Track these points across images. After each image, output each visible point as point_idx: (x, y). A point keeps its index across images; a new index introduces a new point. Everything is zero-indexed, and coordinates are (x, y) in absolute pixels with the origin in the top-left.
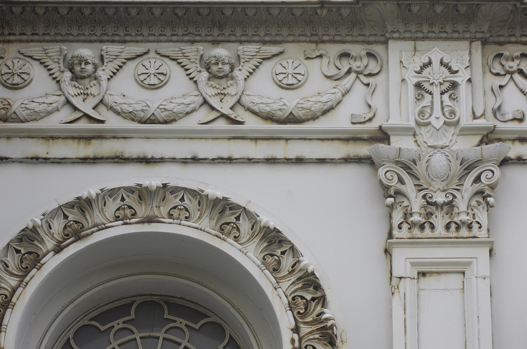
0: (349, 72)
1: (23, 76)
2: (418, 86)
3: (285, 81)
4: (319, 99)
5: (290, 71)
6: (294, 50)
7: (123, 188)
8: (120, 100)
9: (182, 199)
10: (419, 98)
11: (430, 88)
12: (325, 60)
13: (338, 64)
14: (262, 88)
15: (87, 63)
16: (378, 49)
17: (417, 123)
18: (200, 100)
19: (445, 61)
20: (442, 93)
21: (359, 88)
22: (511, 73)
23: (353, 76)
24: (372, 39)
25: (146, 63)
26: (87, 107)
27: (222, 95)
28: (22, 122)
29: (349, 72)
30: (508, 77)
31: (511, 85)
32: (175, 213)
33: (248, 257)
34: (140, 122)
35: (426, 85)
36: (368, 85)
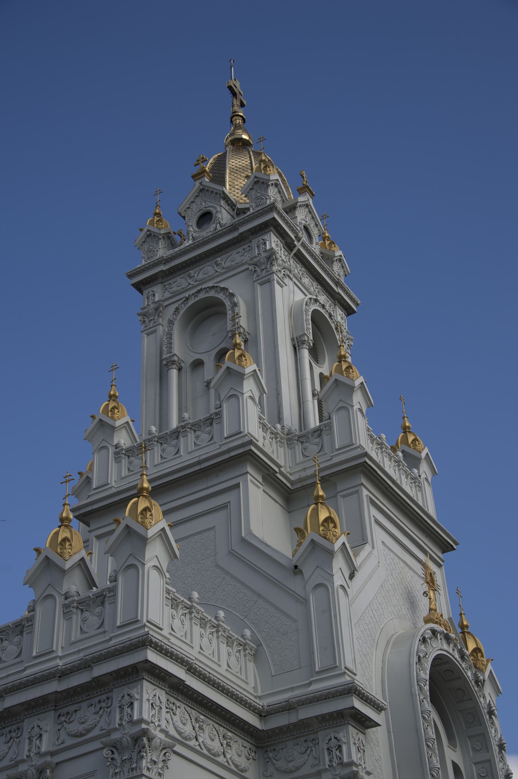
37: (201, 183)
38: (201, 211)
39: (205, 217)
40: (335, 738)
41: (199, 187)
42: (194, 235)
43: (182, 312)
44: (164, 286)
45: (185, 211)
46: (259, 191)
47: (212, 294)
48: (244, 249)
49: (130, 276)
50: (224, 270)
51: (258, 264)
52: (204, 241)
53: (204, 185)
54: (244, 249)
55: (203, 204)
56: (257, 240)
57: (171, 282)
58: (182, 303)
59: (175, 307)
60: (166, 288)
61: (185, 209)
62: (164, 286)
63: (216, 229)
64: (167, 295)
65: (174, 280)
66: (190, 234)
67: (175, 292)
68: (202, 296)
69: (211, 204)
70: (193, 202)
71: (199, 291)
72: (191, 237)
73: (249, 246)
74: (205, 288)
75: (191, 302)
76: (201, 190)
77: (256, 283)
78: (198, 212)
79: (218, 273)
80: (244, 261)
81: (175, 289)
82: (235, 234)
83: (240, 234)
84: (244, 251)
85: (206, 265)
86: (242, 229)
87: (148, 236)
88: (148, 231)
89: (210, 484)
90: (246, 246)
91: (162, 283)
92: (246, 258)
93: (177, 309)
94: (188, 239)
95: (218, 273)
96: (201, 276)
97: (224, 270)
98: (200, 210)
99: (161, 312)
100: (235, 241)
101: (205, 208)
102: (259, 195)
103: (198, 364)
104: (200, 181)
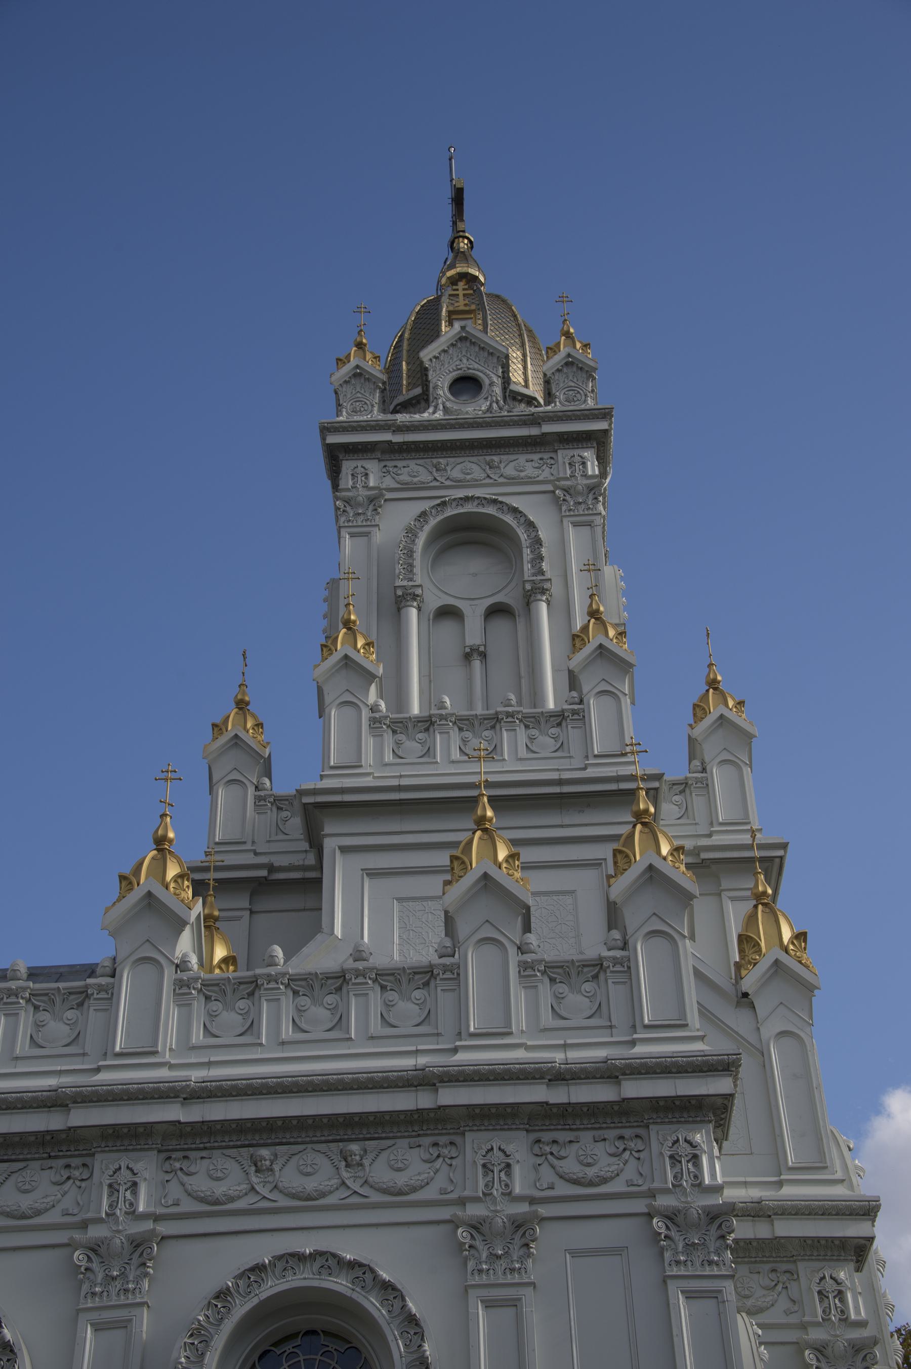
0: (438, 1156)
1: (224, 1171)
2: (484, 1166)
3: (396, 1166)
4: (418, 1177)
5: (400, 1158)
6: (403, 1143)
7: (288, 1254)
8: (287, 1185)
9: (327, 1260)
10: (485, 1175)
11: (491, 1167)
12: (422, 1149)
13: (431, 1150)
14: (380, 1171)
15: (265, 1160)
16: (458, 1139)
17: (483, 1193)
18: (339, 1181)
19: (502, 1147)
20: (500, 1171)
21: (445, 1167)
22: (546, 1155)
23: (441, 1159)
24: (451, 1131)
25: (305, 1157)
26: (265, 1192)
27: (356, 1178)
28: (222, 1204)
29: (438, 1156)
30: (544, 1157)
31: (546, 1163)
32: (323, 1271)
33: (373, 1304)
34: (300, 1199)
35: (489, 1166)
36: (451, 1165)
37: (463, 328)
38: (459, 372)
39: (466, 384)
40: (831, 1278)
41: (459, 333)
42: (448, 404)
43: (433, 522)
44: (385, 466)
45: (431, 360)
46: (571, 378)
47: (491, 510)
48: (541, 459)
49: (325, 430)
50: (501, 480)
51: (572, 491)
52: (476, 423)
53: (468, 332)
54: (541, 459)
55: (465, 361)
56: (570, 453)
57: (400, 464)
58: (433, 507)
59: (423, 509)
60: (389, 472)
61: (431, 356)
62: (385, 466)
63: (490, 409)
64: (389, 482)
65: (404, 463)
66: (440, 401)
67: (406, 484)
68: (469, 508)
69: (480, 367)
70: (444, 351)
71: (467, 499)
72: (441, 407)
73: (551, 458)
74: (501, 502)
75: (450, 512)
76: (461, 339)
77: (565, 520)
78: (454, 371)
79: (491, 481)
80: (541, 478)
81: (405, 478)
82: (534, 431)
83: (543, 434)
84: (541, 462)
85: (467, 459)
86: (547, 428)
87: (356, 375)
88: (357, 367)
89: (567, 821)
90: (546, 456)
91: (380, 460)
92: (545, 474)
93: (423, 515)
94: (436, 407)
95: (491, 481)
96: (456, 473)
97: (501, 480)
98: (458, 369)
99: (380, 507)
100: (529, 441)
101: (469, 369)
102: (573, 384)
103: (448, 613)
104: (463, 323)
